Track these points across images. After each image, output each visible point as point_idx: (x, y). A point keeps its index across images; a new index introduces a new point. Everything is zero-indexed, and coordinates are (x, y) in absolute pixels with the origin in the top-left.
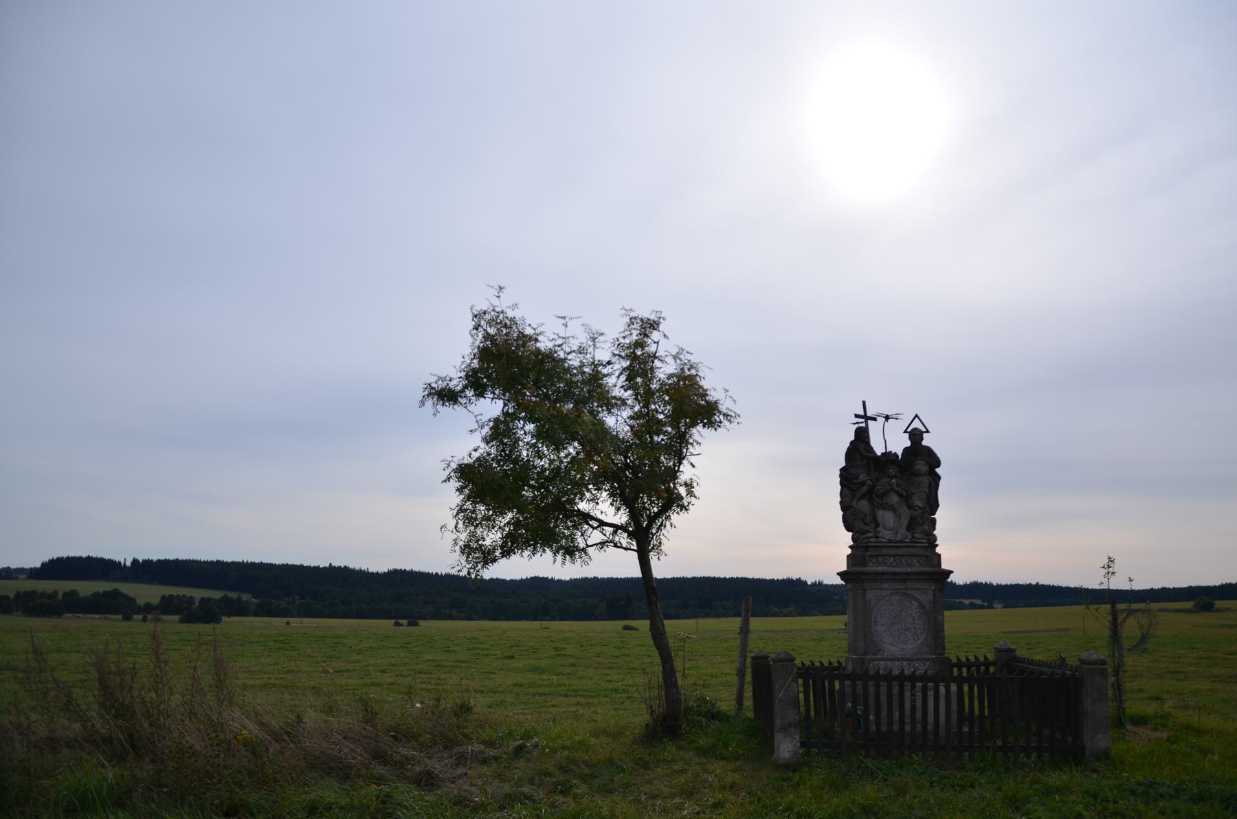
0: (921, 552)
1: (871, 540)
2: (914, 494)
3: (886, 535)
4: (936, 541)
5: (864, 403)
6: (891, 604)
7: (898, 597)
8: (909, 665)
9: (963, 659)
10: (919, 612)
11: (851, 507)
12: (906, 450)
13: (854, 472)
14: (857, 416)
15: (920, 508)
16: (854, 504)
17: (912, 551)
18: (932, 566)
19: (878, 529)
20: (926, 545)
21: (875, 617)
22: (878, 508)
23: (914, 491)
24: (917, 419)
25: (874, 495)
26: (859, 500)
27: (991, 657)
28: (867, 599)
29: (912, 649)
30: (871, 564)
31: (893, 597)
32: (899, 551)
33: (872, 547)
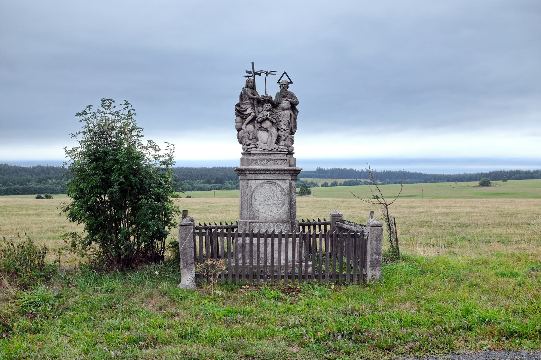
1: (253, 149)
2: (281, 121)
3: (262, 146)
4: (293, 150)
5: (253, 64)
6: (264, 189)
8: (274, 225)
9: (312, 221)
10: (281, 193)
11: (242, 129)
12: (278, 94)
13: (244, 107)
14: (247, 72)
15: (285, 130)
16: (244, 127)
17: (279, 156)
18: (290, 166)
19: (258, 143)
20: (287, 153)
21: (254, 197)
22: (258, 130)
23: (281, 120)
25: (256, 122)
26: (247, 125)
27: (328, 220)
28: (249, 185)
29: (276, 216)
32: (270, 157)
33: (253, 154)
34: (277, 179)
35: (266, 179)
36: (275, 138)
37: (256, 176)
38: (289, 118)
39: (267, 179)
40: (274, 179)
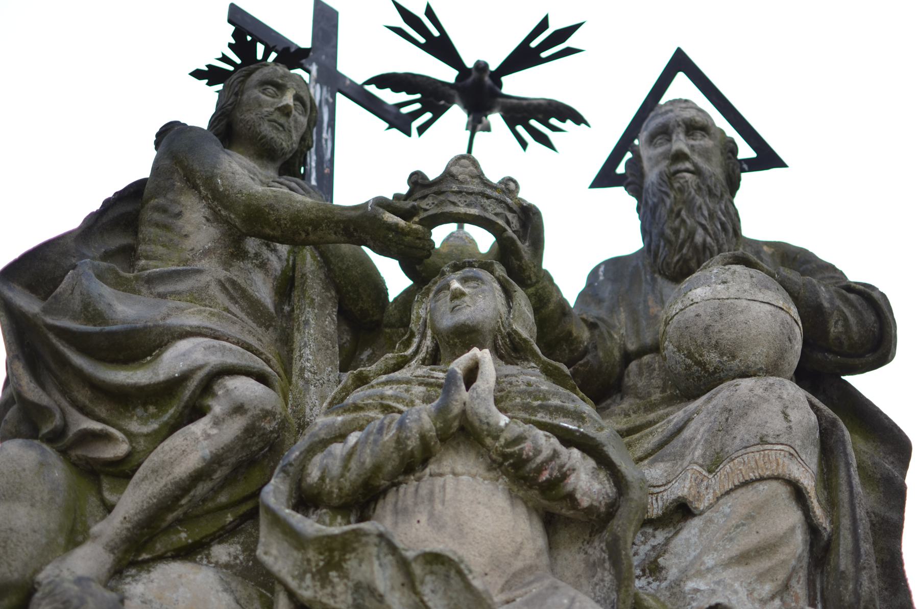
23: (681, 489)
38: (812, 458)
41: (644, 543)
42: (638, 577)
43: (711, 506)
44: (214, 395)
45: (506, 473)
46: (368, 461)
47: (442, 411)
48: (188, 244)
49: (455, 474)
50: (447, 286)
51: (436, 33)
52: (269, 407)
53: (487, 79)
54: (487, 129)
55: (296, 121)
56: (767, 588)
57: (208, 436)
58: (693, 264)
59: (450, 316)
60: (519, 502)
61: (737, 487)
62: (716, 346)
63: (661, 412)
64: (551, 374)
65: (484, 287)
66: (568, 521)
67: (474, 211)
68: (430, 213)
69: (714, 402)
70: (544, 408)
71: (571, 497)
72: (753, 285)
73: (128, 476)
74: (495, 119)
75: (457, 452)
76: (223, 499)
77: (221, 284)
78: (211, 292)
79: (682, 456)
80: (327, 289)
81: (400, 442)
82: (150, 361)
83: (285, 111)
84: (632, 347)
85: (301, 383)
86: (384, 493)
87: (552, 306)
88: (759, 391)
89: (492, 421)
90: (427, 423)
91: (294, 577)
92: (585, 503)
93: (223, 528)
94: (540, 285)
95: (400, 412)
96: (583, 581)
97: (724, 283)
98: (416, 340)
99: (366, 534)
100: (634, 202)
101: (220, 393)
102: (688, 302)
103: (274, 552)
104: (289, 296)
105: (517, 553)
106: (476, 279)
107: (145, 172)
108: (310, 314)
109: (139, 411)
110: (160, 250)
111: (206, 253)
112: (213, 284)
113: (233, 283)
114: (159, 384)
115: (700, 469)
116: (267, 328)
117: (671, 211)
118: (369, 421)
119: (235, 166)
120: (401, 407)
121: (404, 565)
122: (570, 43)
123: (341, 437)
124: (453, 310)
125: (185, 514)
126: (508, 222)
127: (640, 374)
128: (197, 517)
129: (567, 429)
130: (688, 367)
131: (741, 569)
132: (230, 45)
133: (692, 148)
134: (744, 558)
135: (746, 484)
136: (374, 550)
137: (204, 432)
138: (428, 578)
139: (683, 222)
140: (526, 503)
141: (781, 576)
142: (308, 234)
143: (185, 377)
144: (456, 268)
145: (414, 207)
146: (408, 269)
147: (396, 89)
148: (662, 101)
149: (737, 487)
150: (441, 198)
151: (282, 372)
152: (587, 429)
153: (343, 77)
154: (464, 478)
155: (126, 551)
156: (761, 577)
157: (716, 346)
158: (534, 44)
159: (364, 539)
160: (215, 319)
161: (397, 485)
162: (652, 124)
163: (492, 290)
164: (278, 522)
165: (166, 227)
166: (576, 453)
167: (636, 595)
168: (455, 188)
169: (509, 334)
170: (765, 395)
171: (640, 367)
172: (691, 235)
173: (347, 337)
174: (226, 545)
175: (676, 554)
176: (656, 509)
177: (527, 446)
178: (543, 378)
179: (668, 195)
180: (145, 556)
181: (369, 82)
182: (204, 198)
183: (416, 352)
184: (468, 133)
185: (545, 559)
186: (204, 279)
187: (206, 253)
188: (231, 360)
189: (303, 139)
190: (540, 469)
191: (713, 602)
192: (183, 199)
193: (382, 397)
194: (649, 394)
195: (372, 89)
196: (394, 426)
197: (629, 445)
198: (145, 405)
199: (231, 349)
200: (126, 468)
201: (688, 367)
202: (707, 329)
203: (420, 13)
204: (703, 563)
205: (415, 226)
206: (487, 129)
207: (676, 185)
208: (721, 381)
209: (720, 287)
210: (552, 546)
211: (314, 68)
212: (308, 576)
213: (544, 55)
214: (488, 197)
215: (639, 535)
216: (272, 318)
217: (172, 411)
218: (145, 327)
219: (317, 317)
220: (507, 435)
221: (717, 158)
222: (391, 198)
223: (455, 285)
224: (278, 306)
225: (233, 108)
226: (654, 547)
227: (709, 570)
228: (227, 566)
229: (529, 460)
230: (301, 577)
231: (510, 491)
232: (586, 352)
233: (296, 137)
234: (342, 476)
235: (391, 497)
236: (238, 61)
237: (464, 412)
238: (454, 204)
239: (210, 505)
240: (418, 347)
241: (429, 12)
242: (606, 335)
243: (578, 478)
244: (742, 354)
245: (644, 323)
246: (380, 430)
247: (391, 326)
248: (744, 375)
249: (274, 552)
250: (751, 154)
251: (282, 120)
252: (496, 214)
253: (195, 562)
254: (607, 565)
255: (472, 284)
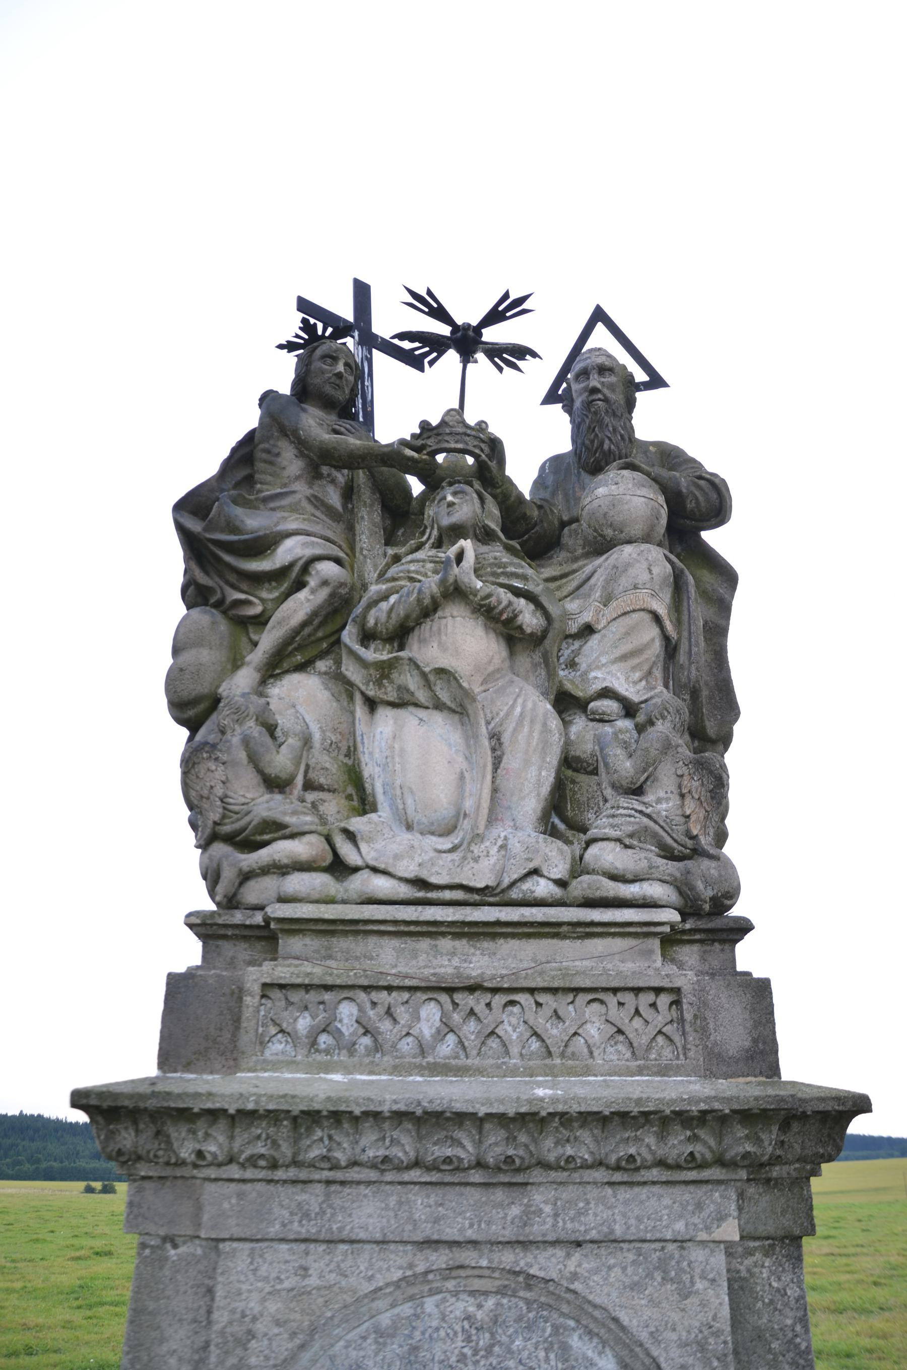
0: (629, 966)
1: (297, 883)
2: (588, 630)
4: (731, 894)
7: (463, 1305)
15: (629, 709)
20: (673, 916)
22: (372, 704)
23: (587, 617)
24: (600, 327)
28: (221, 1317)
30: (278, 1047)
31: (430, 1304)
34: (569, 1227)
35: (427, 1231)
36: (532, 772)
37: (312, 1197)
39: (451, 1233)
40: (540, 1228)
41: (567, 649)
42: (563, 670)
43: (605, 627)
44: (310, 574)
45: (482, 614)
46: (402, 613)
47: (443, 581)
48: (286, 473)
49: (453, 617)
50: (445, 498)
51: (435, 305)
52: (342, 581)
53: (471, 333)
54: (476, 362)
55: (347, 380)
56: (637, 675)
57: (308, 600)
58: (603, 463)
59: (446, 517)
60: (491, 631)
61: (620, 616)
62: (611, 525)
63: (581, 563)
64: (509, 549)
65: (467, 498)
66: (521, 640)
67: (460, 446)
68: (433, 448)
69: (609, 561)
70: (504, 574)
71: (520, 628)
72: (634, 485)
73: (265, 623)
74: (480, 356)
75: (454, 603)
76: (320, 634)
77: (308, 499)
78: (303, 505)
79: (589, 596)
80: (374, 493)
81: (419, 600)
82: (270, 554)
83: (339, 375)
84: (565, 518)
85: (361, 557)
86: (413, 629)
87: (512, 499)
88: (634, 556)
89: (472, 586)
90: (435, 589)
91: (363, 684)
92: (529, 631)
93: (321, 651)
94: (504, 487)
95: (420, 581)
96: (530, 674)
97: (616, 484)
98: (428, 531)
99: (402, 659)
100: (566, 418)
101: (313, 573)
102: (594, 497)
103: (351, 669)
104: (351, 498)
105: (490, 662)
106: (462, 492)
107: (254, 423)
108: (363, 512)
109: (267, 585)
110: (269, 478)
111: (297, 478)
112: (303, 499)
113: (316, 497)
114: (277, 570)
115: (598, 604)
116: (339, 522)
117: (589, 427)
118: (402, 587)
119: (311, 422)
120: (419, 577)
121: (424, 675)
122: (525, 306)
123: (385, 597)
124: (448, 514)
125: (299, 645)
126: (482, 450)
127: (570, 536)
128: (306, 646)
129: (517, 587)
130: (595, 538)
131: (622, 665)
132: (300, 328)
133: (603, 383)
134: (624, 658)
135: (625, 614)
136: (407, 668)
137: (306, 598)
138: (438, 682)
139: (596, 435)
140: (495, 631)
141: (646, 668)
142: (359, 463)
143: (291, 565)
144: (451, 484)
145: (423, 445)
146: (422, 480)
147: (412, 341)
148: (584, 350)
149: (620, 616)
150: (440, 438)
151: (348, 551)
152: (530, 587)
153: (377, 336)
154: (458, 619)
155: (267, 670)
156: (633, 669)
157: (611, 525)
158: (500, 308)
159: (401, 662)
160: (306, 522)
161: (420, 624)
162: (577, 367)
163: (472, 499)
164: (351, 652)
165: (271, 463)
166: (522, 601)
167: (560, 682)
168: (448, 431)
169: (483, 527)
170: (638, 558)
171: (570, 530)
172: (602, 444)
173: (388, 522)
174: (324, 661)
175: (585, 656)
176: (573, 628)
177: (493, 600)
178: (504, 553)
179: (587, 417)
180: (278, 671)
181: (393, 337)
182: (293, 442)
183: (429, 538)
184: (461, 365)
185: (507, 663)
186: (297, 496)
187: (297, 478)
188: (318, 551)
189: (352, 390)
190: (501, 613)
191: (604, 685)
192: (280, 444)
193: (409, 572)
194: (575, 550)
195: (396, 341)
196: (416, 591)
197: (559, 588)
198: (269, 581)
199: (317, 543)
200: (262, 619)
201: (595, 538)
202: (605, 514)
203: (423, 293)
204: (600, 661)
205: (424, 457)
206: (476, 362)
207: (593, 410)
208: (615, 546)
209: (614, 487)
210: (512, 653)
211: (356, 334)
212: (371, 683)
213: (508, 314)
214: (469, 435)
215: (564, 644)
216: (341, 516)
217: (286, 585)
218: (265, 534)
219: (369, 513)
220: (482, 594)
221: (620, 389)
222: (409, 438)
223: (450, 498)
224: (344, 506)
225: (306, 375)
226: (573, 651)
227: (603, 665)
228: (325, 673)
229: (495, 607)
230: (367, 684)
231: (485, 625)
232: (536, 524)
233: (347, 391)
234: (387, 622)
235: (416, 632)
236: (306, 337)
237: (456, 581)
238: (447, 441)
239: (313, 638)
240: (430, 535)
241: (429, 293)
242: (548, 511)
243: (524, 617)
244: (627, 530)
245: (573, 502)
246: (409, 594)
247: (415, 514)
248: (629, 542)
249: (351, 669)
250: (646, 378)
251: (338, 382)
252: (474, 446)
253: (307, 672)
254: (543, 666)
255: (460, 496)
